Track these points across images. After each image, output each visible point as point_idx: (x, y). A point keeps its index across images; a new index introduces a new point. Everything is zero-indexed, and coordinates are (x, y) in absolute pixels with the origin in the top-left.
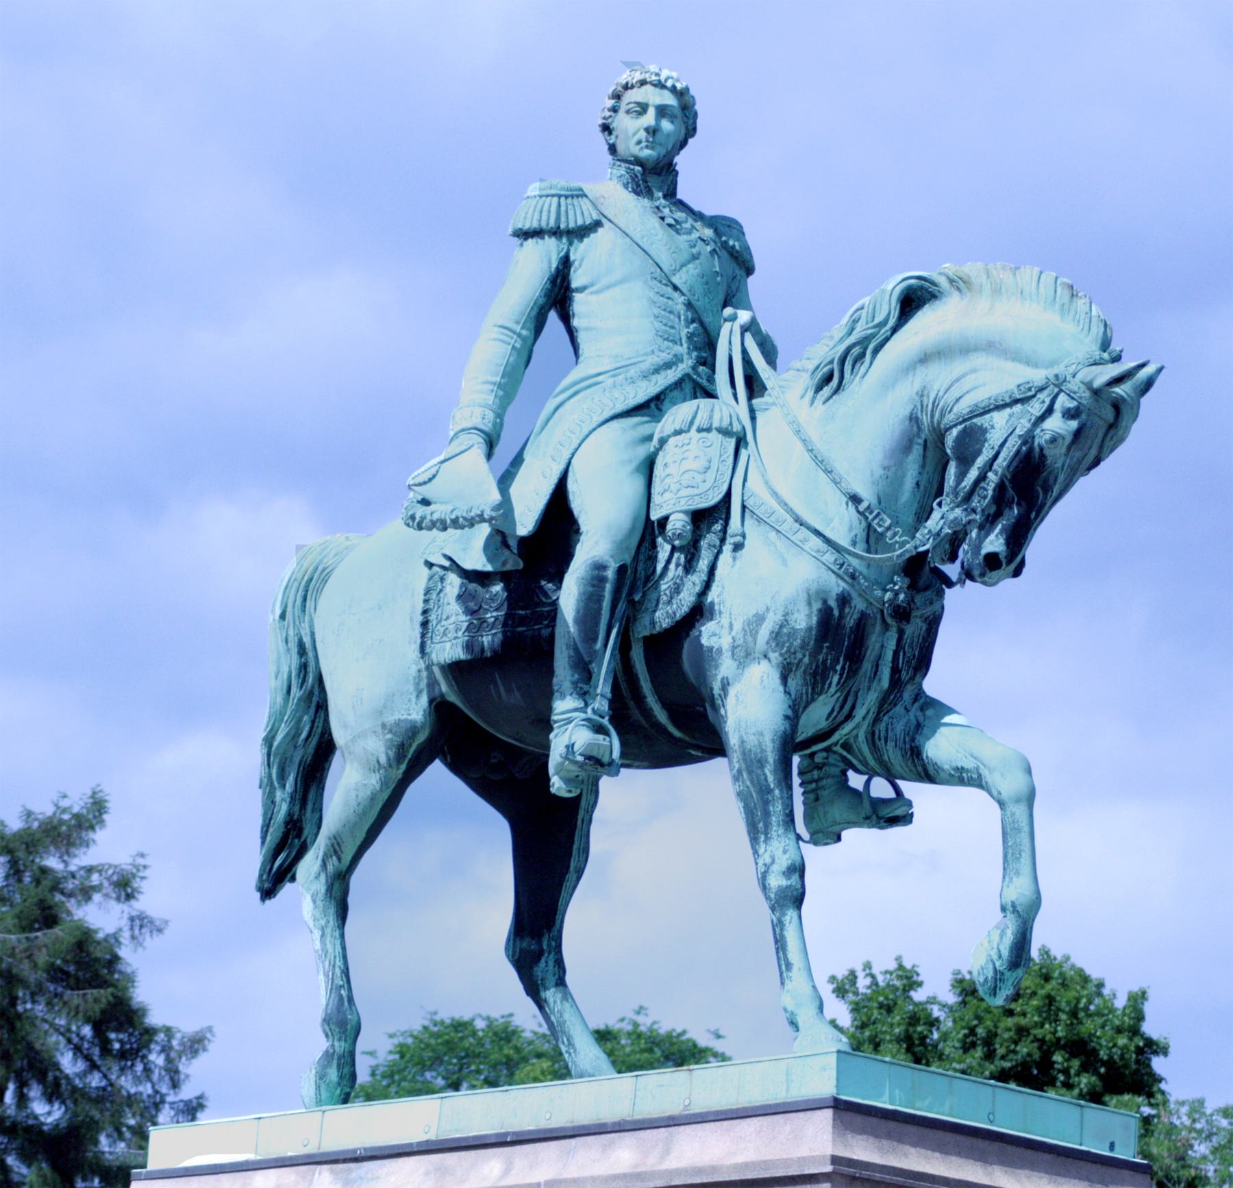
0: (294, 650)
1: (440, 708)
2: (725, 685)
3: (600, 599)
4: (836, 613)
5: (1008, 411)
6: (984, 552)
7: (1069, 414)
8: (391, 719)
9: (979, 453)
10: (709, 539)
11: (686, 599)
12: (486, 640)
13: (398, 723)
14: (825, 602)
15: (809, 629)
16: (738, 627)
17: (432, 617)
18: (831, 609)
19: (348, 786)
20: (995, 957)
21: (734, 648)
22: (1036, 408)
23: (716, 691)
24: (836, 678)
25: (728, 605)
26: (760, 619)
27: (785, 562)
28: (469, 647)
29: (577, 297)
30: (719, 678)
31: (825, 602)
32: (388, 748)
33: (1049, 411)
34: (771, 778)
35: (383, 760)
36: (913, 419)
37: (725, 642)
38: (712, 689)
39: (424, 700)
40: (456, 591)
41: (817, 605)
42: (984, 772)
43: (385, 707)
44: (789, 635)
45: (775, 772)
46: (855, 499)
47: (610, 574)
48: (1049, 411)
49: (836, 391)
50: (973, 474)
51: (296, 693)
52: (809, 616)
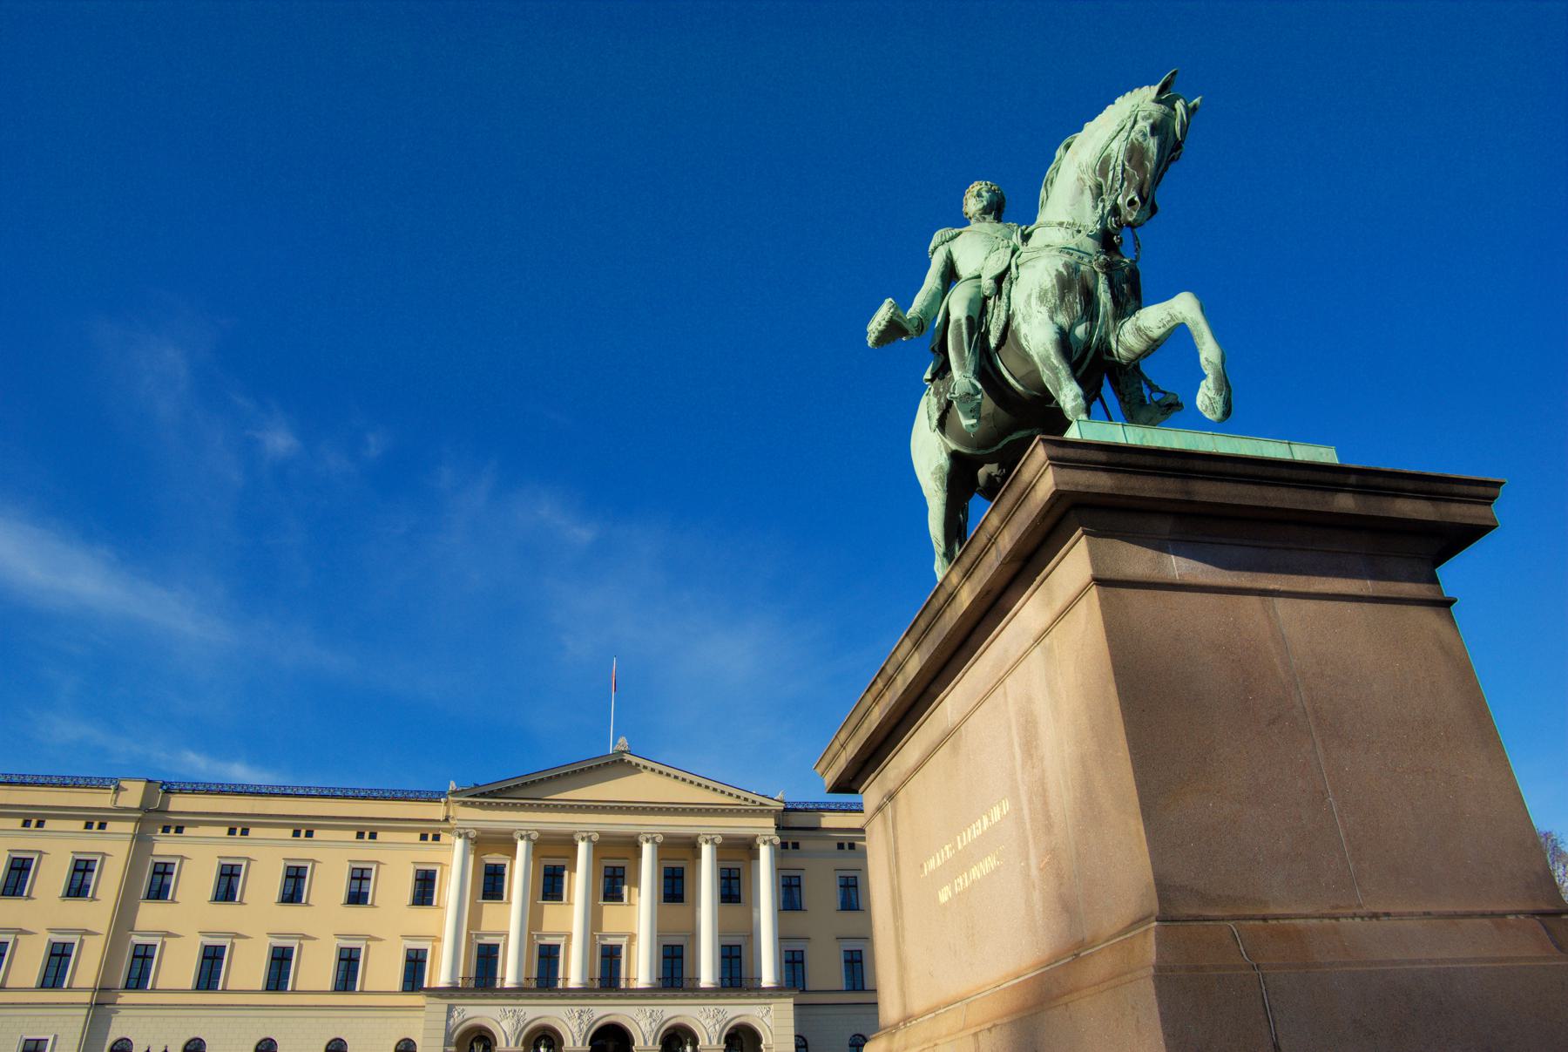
1: (954, 456)
7: (1145, 118)
10: (1005, 285)
26: (1029, 296)
33: (1135, 122)
36: (1080, 179)
39: (945, 455)
41: (1054, 273)
46: (1061, 224)
47: (964, 321)
48: (1135, 122)
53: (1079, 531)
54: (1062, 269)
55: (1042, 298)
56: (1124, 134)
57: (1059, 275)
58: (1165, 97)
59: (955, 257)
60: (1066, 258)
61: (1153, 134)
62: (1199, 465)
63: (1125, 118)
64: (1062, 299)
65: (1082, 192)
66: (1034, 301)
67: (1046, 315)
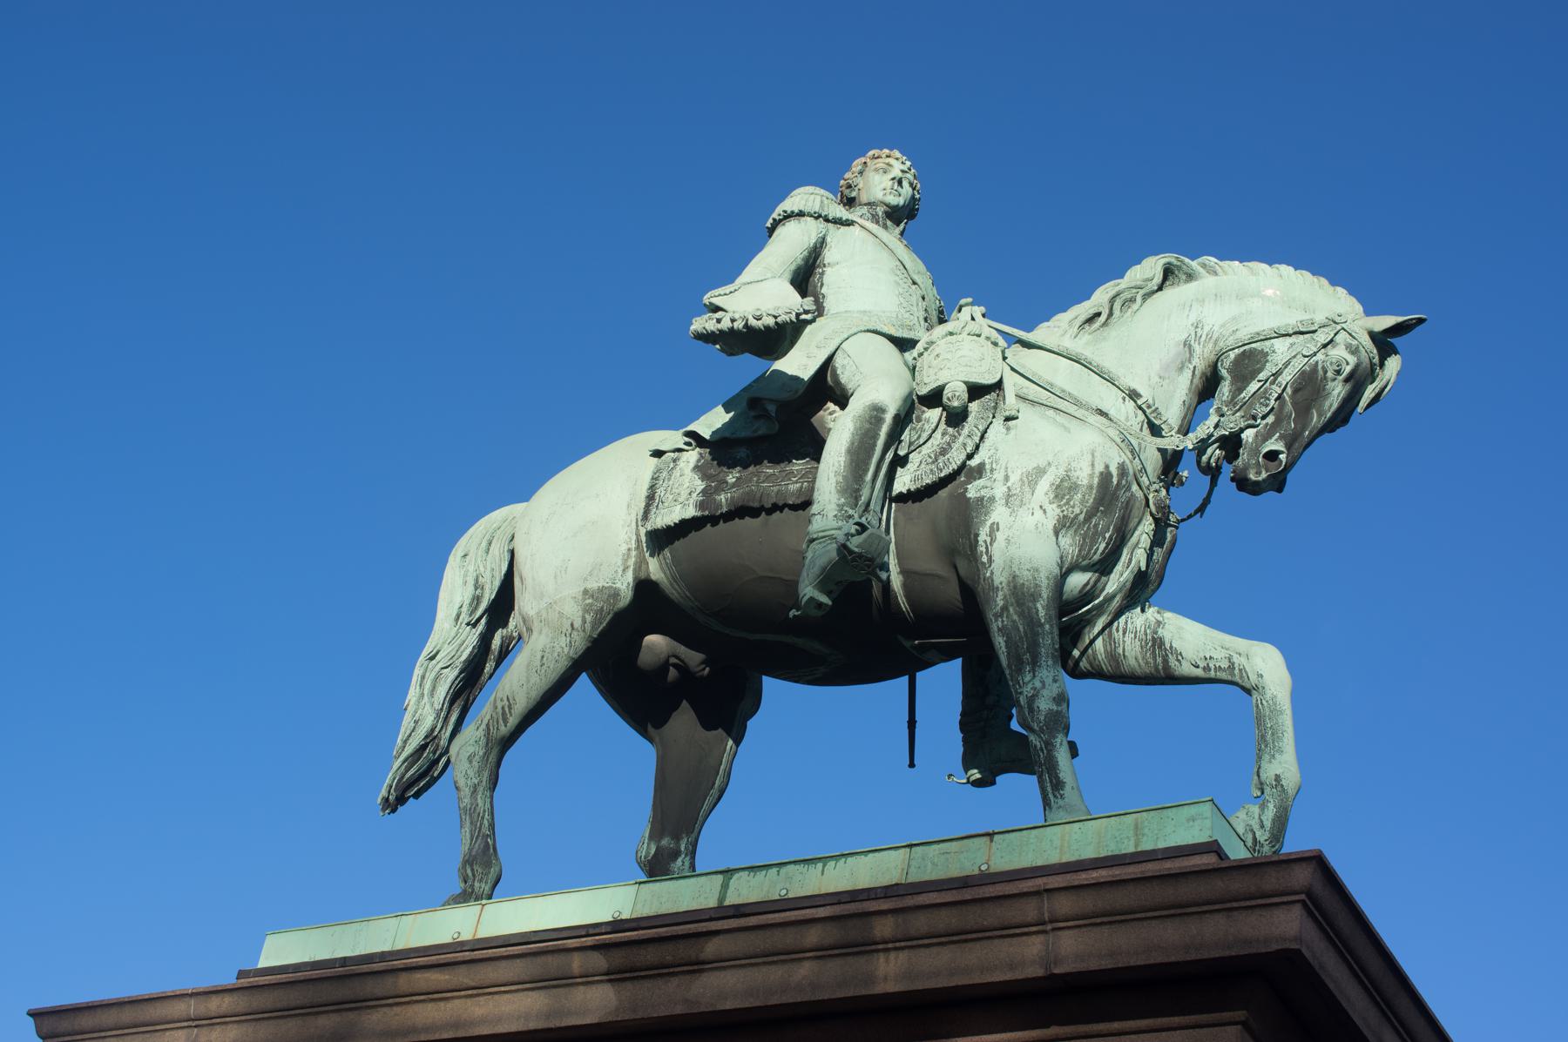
0: (471, 582)
1: (644, 587)
2: (995, 528)
3: (875, 437)
4: (1115, 480)
5: (1289, 340)
6: (1265, 450)
8: (593, 585)
9: (1260, 370)
11: (956, 457)
12: (722, 498)
13: (601, 590)
14: (1107, 467)
15: (1091, 487)
16: (1014, 478)
17: (660, 492)
18: (1111, 476)
19: (517, 682)
20: (1256, 827)
21: (1008, 496)
22: (1322, 337)
23: (983, 536)
24: (1103, 545)
25: (1003, 462)
26: (1040, 472)
27: (1067, 430)
28: (701, 505)
29: (828, 270)
30: (988, 523)
31: (1107, 467)
32: (586, 611)
34: (1042, 613)
35: (578, 624)
37: (999, 491)
38: (977, 535)
39: (629, 577)
40: (692, 465)
41: (1100, 468)
42: (1236, 659)
43: (591, 574)
44: (1070, 488)
45: (1047, 608)
46: (1133, 395)
47: (888, 418)
49: (1105, 324)
50: (1254, 386)
51: (465, 618)
52: (1091, 476)
53: (1240, 1015)
54: (1114, 471)
55: (1063, 490)
56: (1306, 345)
57: (1106, 476)
58: (1384, 342)
59: (829, 256)
60: (1125, 457)
61: (1346, 380)
62: (1403, 1004)
63: (1279, 307)
64: (1089, 516)
65: (1181, 369)
66: (1044, 485)
67: (1050, 523)
